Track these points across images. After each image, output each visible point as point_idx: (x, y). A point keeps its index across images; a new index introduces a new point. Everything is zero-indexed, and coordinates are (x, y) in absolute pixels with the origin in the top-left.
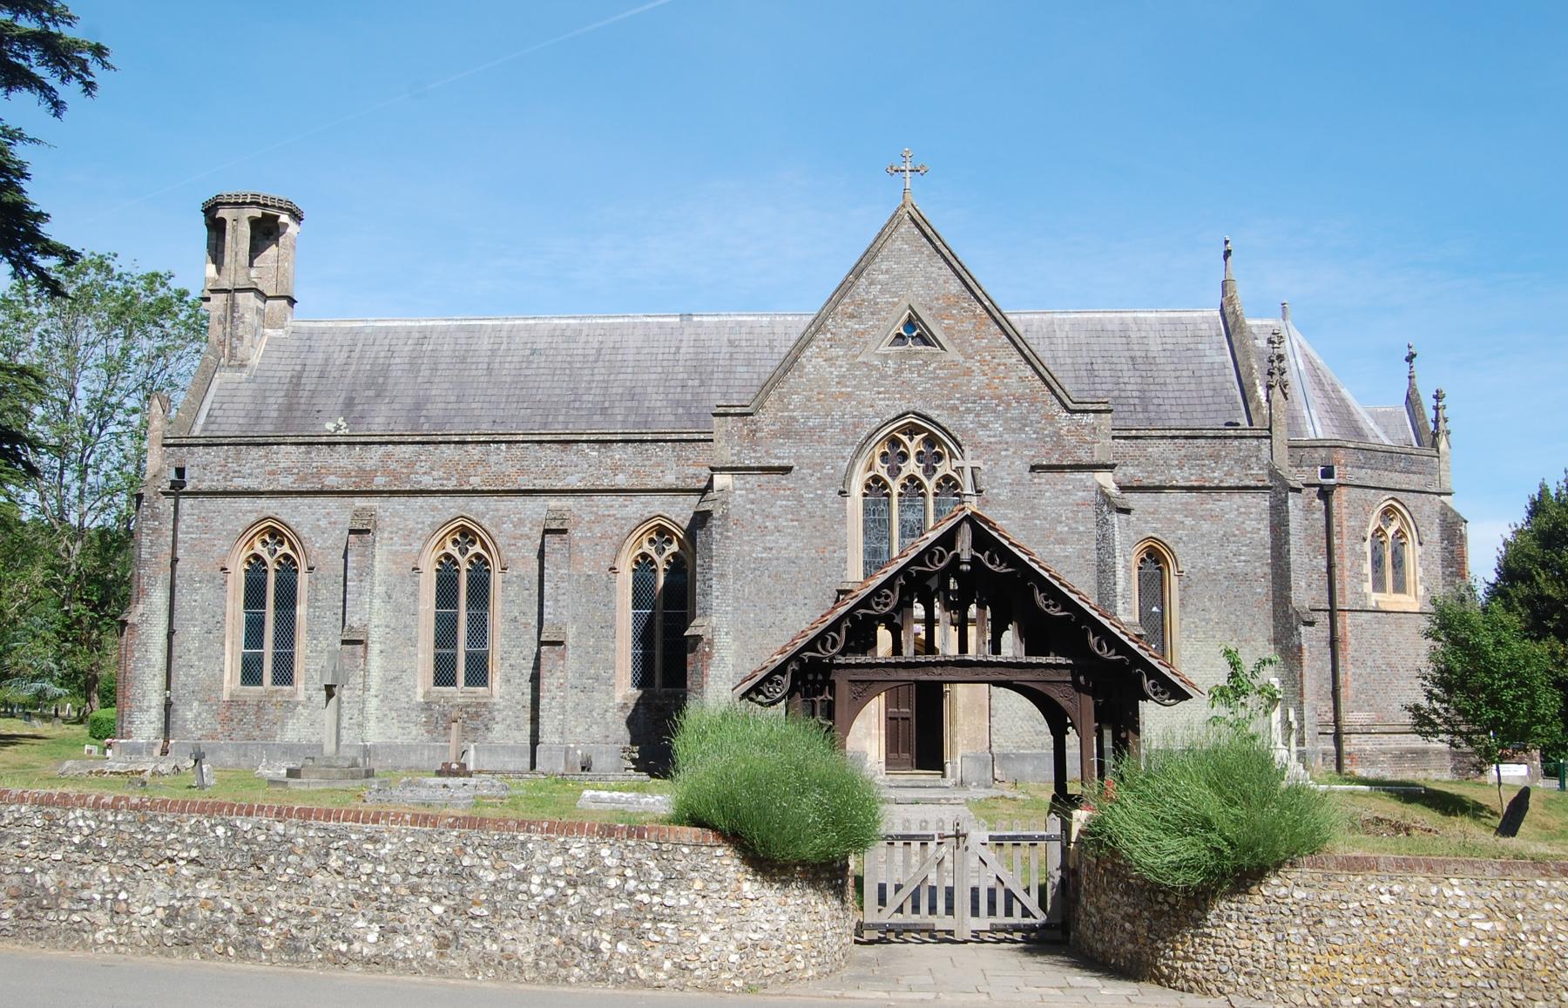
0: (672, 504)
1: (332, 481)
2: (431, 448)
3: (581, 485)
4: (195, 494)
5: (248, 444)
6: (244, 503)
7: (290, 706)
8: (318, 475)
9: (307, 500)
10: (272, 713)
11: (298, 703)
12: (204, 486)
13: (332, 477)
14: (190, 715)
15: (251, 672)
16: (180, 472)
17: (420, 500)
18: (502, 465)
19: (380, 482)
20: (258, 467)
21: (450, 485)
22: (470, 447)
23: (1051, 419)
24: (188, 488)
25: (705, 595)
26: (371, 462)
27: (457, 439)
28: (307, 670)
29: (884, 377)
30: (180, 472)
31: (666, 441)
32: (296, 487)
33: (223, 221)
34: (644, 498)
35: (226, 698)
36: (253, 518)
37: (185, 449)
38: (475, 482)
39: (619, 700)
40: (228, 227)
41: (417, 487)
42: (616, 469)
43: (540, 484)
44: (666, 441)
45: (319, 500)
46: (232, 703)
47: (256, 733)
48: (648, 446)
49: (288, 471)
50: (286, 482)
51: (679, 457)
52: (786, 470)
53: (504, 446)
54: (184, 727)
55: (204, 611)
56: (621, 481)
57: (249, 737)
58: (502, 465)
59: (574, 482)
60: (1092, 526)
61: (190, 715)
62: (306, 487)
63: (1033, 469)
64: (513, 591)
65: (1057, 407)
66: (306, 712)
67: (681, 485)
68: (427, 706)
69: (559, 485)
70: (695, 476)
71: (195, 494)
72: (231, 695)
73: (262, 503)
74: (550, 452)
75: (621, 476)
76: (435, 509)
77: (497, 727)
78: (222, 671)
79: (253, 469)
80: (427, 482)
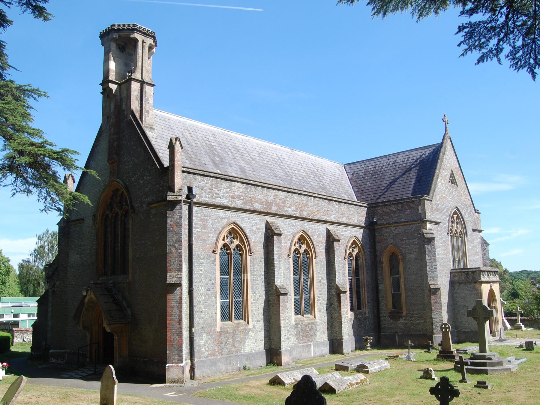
0: (357, 232)
1: (257, 206)
2: (290, 194)
3: (334, 220)
4: (199, 204)
5: (222, 179)
6: (221, 213)
7: (246, 332)
8: (250, 201)
9: (248, 215)
10: (240, 336)
11: (249, 330)
12: (203, 200)
13: (257, 204)
14: (202, 342)
15: (226, 316)
16: (190, 189)
17: (288, 221)
18: (312, 208)
19: (274, 209)
20: (227, 193)
21: (298, 214)
22: (302, 197)
23: (473, 213)
24: (195, 200)
25: (432, 271)
26: (271, 198)
27: (299, 192)
28: (252, 311)
29: (450, 193)
30: (190, 189)
31: (354, 205)
32: (242, 207)
33: (136, 41)
34: (350, 228)
35: (219, 330)
36: (225, 222)
37: (192, 176)
38: (305, 214)
39: (349, 317)
40: (140, 44)
41: (287, 214)
42: (343, 214)
43: (324, 218)
44: (354, 205)
45: (252, 216)
46: (223, 332)
47: (233, 349)
48: (350, 206)
49: (239, 196)
50: (238, 204)
51: (357, 212)
52: (438, 223)
53: (312, 198)
54: (199, 351)
55: (206, 277)
56: (344, 220)
57: (230, 352)
58: (312, 208)
59: (332, 218)
60: (480, 250)
61: (202, 342)
62: (247, 207)
63: (473, 230)
64: (319, 266)
65: (474, 211)
66: (253, 334)
67: (358, 224)
68: (296, 326)
69: (329, 219)
70: (361, 221)
71: (199, 204)
72: (221, 328)
73: (229, 214)
74: (325, 203)
75: (344, 218)
76: (293, 226)
77: (318, 333)
78: (216, 313)
79: (224, 193)
80: (290, 212)
